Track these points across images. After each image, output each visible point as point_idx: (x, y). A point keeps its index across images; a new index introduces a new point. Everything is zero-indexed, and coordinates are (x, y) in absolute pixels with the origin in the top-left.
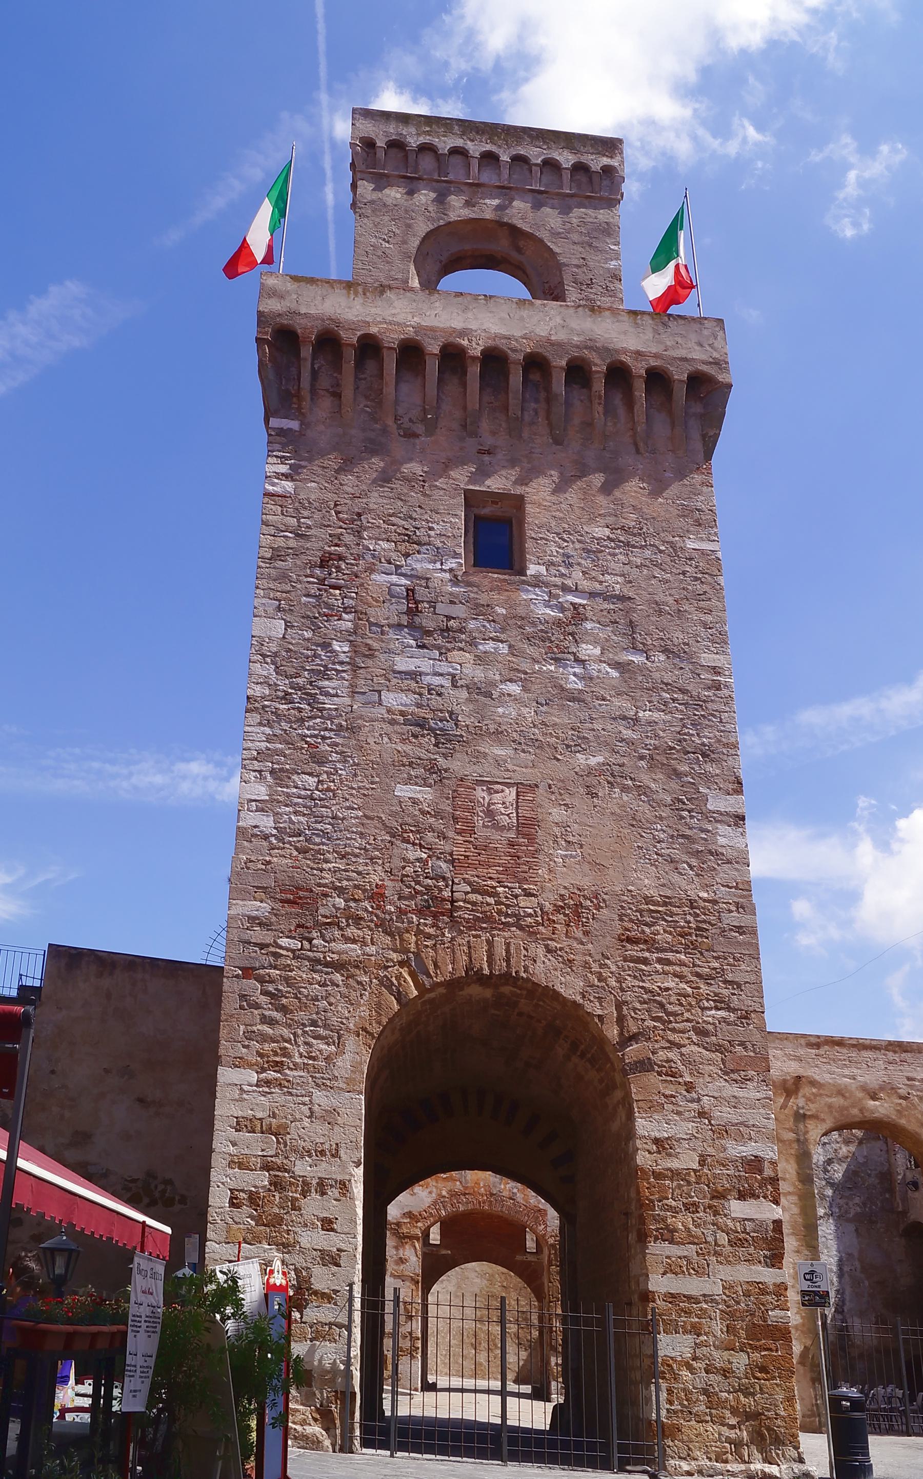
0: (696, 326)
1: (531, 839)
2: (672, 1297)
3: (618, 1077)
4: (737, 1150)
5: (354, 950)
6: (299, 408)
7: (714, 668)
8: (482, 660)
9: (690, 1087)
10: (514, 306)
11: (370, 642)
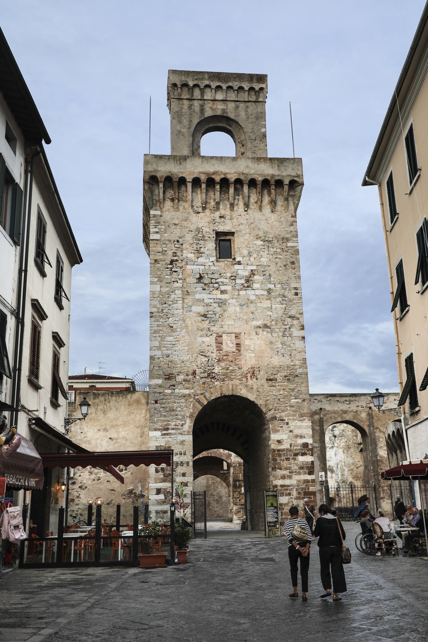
0: (292, 161)
1: (239, 351)
2: (282, 486)
3: (266, 422)
4: (300, 441)
5: (187, 392)
7: (295, 288)
9: (287, 424)
10: (231, 160)
11: (187, 290)
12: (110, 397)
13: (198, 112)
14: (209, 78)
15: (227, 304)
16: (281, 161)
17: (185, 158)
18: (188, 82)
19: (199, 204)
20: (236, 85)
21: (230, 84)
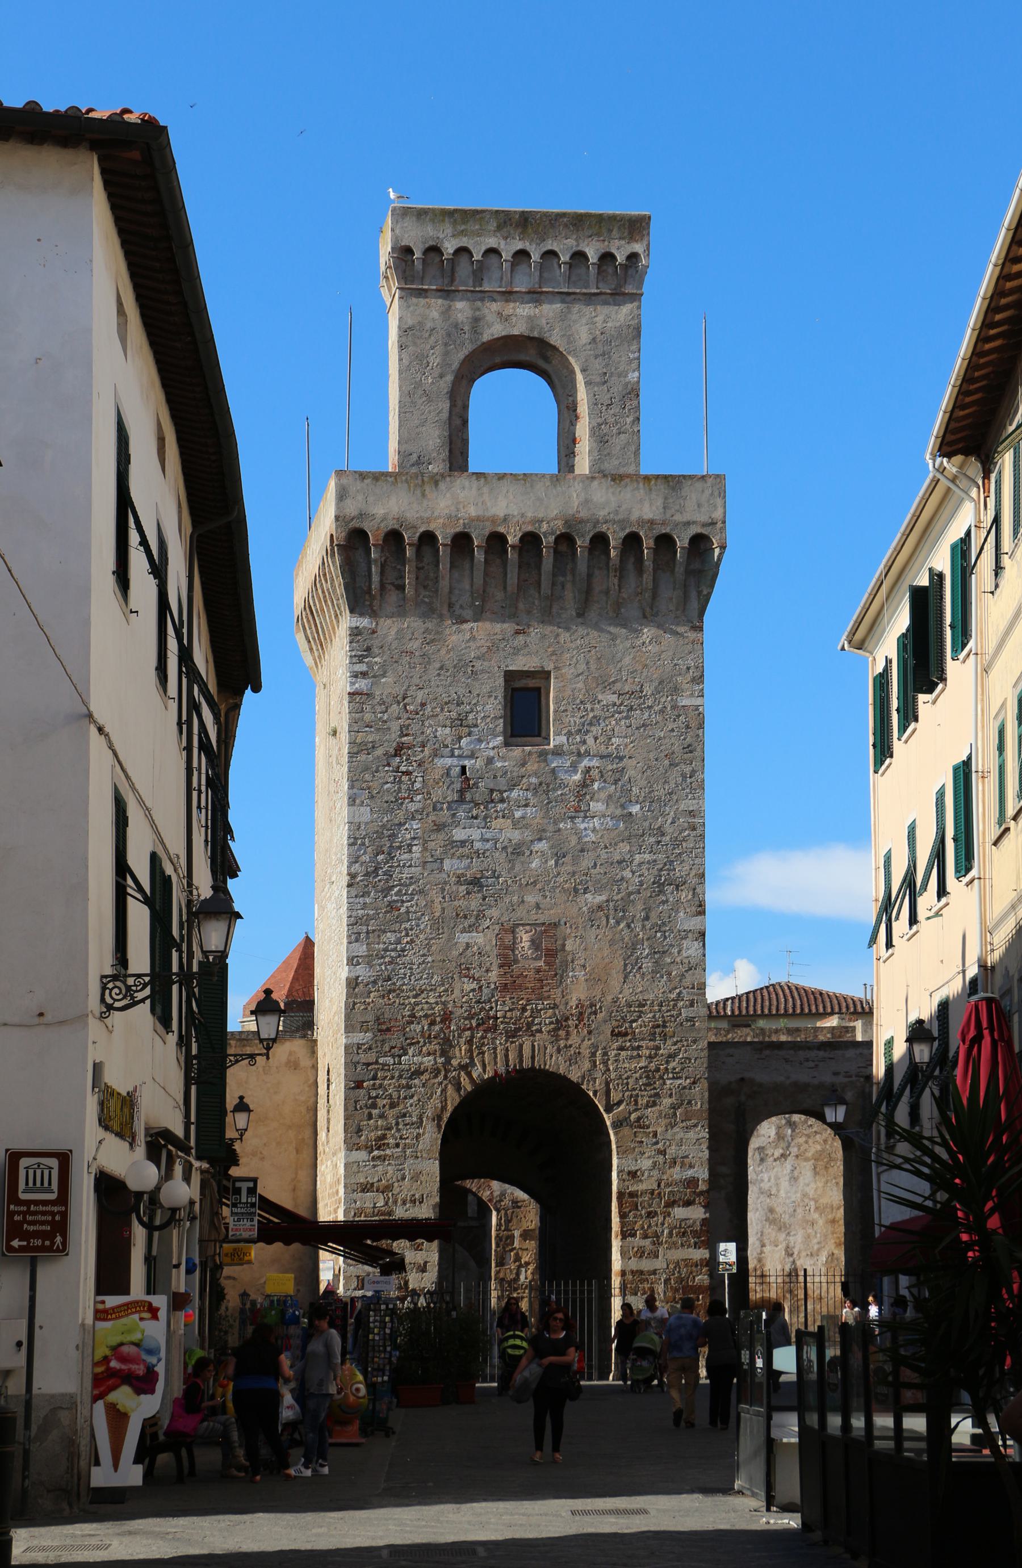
13: (466, 328)
14: (499, 228)
15: (527, 853)
16: (673, 482)
17: (435, 481)
19: (466, 598)
20: (564, 246)
21: (550, 245)
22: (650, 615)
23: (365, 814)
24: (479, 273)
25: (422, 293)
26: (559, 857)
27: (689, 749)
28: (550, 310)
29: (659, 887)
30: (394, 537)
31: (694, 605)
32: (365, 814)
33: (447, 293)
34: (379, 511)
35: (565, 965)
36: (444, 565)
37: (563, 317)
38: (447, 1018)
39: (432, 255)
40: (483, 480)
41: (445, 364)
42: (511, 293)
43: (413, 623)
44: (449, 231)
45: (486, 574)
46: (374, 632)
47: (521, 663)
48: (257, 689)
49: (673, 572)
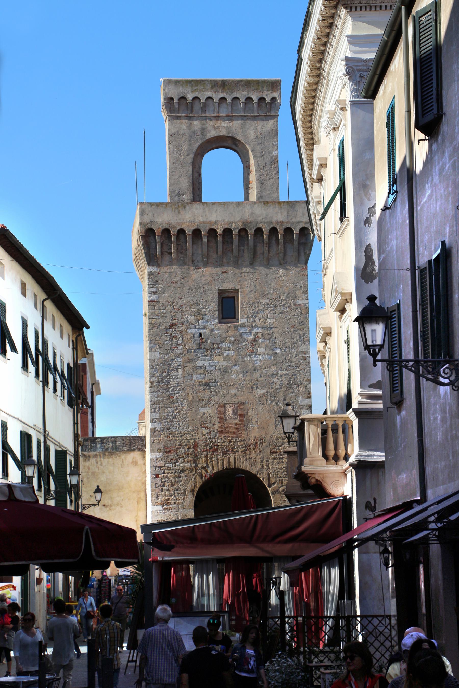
6: (157, 262)
8: (225, 359)
12: (102, 459)
13: (199, 133)
14: (212, 88)
15: (230, 371)
18: (187, 95)
19: (200, 258)
20: (242, 95)
21: (236, 95)
22: (283, 263)
23: (157, 355)
24: (204, 108)
25: (178, 118)
26: (244, 373)
27: (302, 323)
28: (237, 123)
29: (290, 386)
30: (166, 232)
31: (303, 258)
32: (157, 355)
33: (189, 118)
34: (159, 220)
35: (248, 421)
36: (189, 245)
37: (243, 126)
38: (195, 446)
39: (183, 100)
40: (205, 205)
41: (189, 150)
42: (218, 116)
43: (176, 269)
44: (190, 90)
45: (208, 246)
46: (159, 273)
47: (225, 286)
48: (88, 328)
49: (293, 243)
